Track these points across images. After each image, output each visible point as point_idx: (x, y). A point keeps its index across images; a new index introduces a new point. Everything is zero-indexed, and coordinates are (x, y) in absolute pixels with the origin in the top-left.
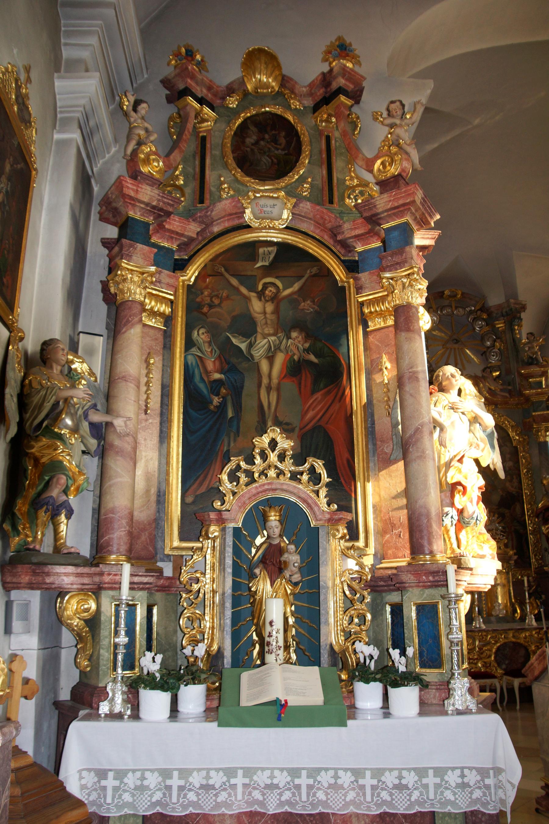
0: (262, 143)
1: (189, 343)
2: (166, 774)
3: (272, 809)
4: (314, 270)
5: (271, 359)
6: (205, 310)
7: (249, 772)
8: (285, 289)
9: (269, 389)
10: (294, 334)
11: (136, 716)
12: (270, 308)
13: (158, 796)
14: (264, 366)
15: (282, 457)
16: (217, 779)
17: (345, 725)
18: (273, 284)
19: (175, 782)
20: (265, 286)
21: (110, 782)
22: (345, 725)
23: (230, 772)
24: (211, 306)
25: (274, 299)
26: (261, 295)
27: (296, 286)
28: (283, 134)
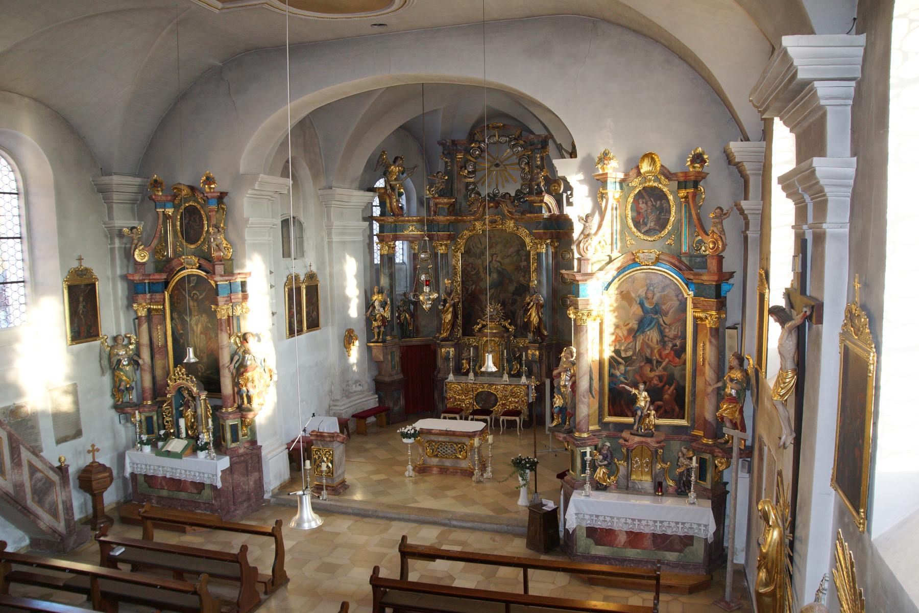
0: (191, 222)
1: (172, 319)
2: (146, 465)
3: (168, 476)
4: (209, 287)
5: (197, 325)
6: (176, 304)
7: (163, 467)
8: (201, 295)
9: (197, 337)
10: (204, 315)
11: (141, 450)
12: (195, 304)
13: (145, 470)
14: (195, 328)
15: (183, 374)
16: (156, 468)
17: (181, 459)
18: (196, 294)
19: (148, 467)
20: (194, 294)
21: (135, 466)
22: (181, 459)
23: (159, 467)
24: (178, 303)
25: (197, 300)
26: (192, 298)
27: (204, 294)
28: (198, 217)
